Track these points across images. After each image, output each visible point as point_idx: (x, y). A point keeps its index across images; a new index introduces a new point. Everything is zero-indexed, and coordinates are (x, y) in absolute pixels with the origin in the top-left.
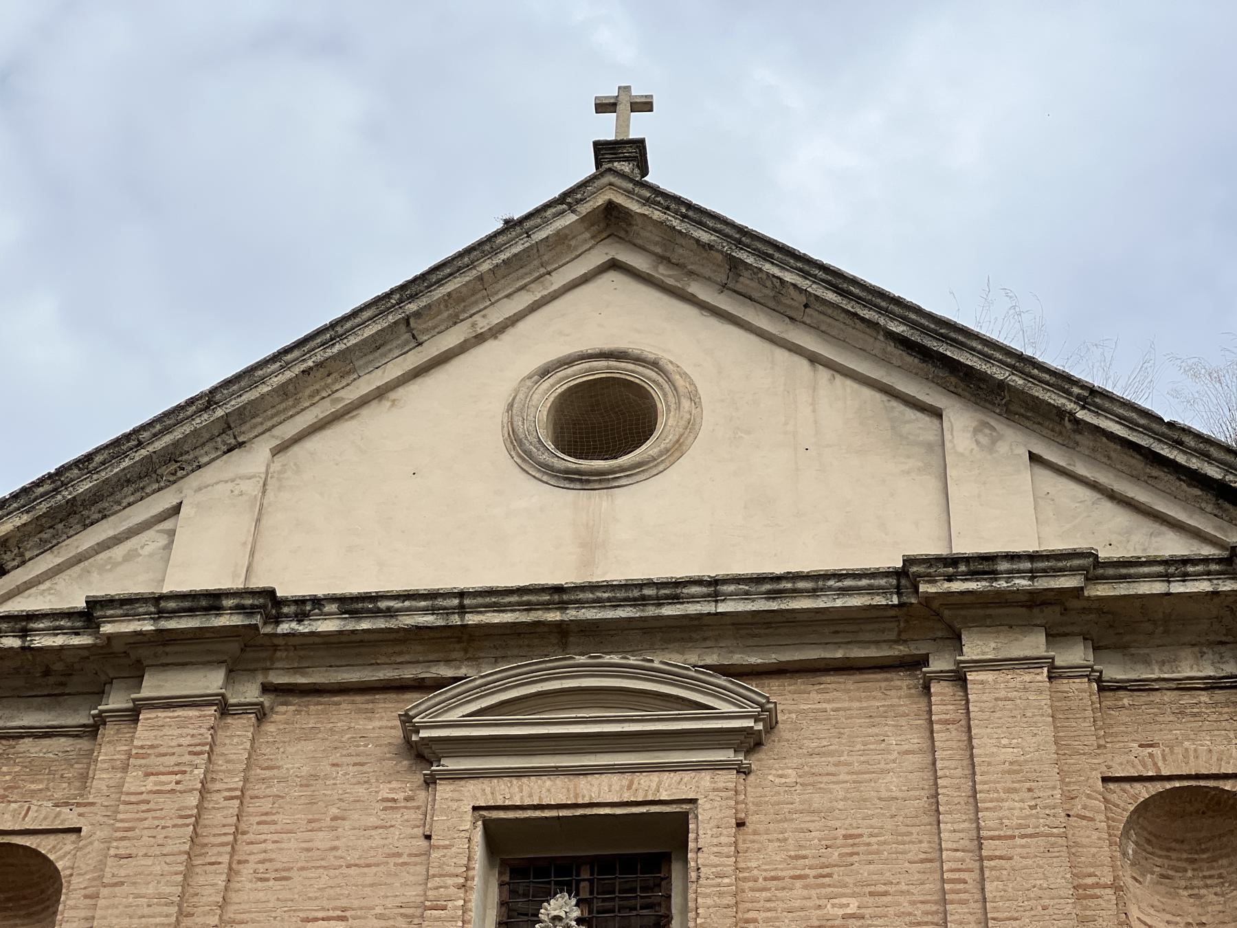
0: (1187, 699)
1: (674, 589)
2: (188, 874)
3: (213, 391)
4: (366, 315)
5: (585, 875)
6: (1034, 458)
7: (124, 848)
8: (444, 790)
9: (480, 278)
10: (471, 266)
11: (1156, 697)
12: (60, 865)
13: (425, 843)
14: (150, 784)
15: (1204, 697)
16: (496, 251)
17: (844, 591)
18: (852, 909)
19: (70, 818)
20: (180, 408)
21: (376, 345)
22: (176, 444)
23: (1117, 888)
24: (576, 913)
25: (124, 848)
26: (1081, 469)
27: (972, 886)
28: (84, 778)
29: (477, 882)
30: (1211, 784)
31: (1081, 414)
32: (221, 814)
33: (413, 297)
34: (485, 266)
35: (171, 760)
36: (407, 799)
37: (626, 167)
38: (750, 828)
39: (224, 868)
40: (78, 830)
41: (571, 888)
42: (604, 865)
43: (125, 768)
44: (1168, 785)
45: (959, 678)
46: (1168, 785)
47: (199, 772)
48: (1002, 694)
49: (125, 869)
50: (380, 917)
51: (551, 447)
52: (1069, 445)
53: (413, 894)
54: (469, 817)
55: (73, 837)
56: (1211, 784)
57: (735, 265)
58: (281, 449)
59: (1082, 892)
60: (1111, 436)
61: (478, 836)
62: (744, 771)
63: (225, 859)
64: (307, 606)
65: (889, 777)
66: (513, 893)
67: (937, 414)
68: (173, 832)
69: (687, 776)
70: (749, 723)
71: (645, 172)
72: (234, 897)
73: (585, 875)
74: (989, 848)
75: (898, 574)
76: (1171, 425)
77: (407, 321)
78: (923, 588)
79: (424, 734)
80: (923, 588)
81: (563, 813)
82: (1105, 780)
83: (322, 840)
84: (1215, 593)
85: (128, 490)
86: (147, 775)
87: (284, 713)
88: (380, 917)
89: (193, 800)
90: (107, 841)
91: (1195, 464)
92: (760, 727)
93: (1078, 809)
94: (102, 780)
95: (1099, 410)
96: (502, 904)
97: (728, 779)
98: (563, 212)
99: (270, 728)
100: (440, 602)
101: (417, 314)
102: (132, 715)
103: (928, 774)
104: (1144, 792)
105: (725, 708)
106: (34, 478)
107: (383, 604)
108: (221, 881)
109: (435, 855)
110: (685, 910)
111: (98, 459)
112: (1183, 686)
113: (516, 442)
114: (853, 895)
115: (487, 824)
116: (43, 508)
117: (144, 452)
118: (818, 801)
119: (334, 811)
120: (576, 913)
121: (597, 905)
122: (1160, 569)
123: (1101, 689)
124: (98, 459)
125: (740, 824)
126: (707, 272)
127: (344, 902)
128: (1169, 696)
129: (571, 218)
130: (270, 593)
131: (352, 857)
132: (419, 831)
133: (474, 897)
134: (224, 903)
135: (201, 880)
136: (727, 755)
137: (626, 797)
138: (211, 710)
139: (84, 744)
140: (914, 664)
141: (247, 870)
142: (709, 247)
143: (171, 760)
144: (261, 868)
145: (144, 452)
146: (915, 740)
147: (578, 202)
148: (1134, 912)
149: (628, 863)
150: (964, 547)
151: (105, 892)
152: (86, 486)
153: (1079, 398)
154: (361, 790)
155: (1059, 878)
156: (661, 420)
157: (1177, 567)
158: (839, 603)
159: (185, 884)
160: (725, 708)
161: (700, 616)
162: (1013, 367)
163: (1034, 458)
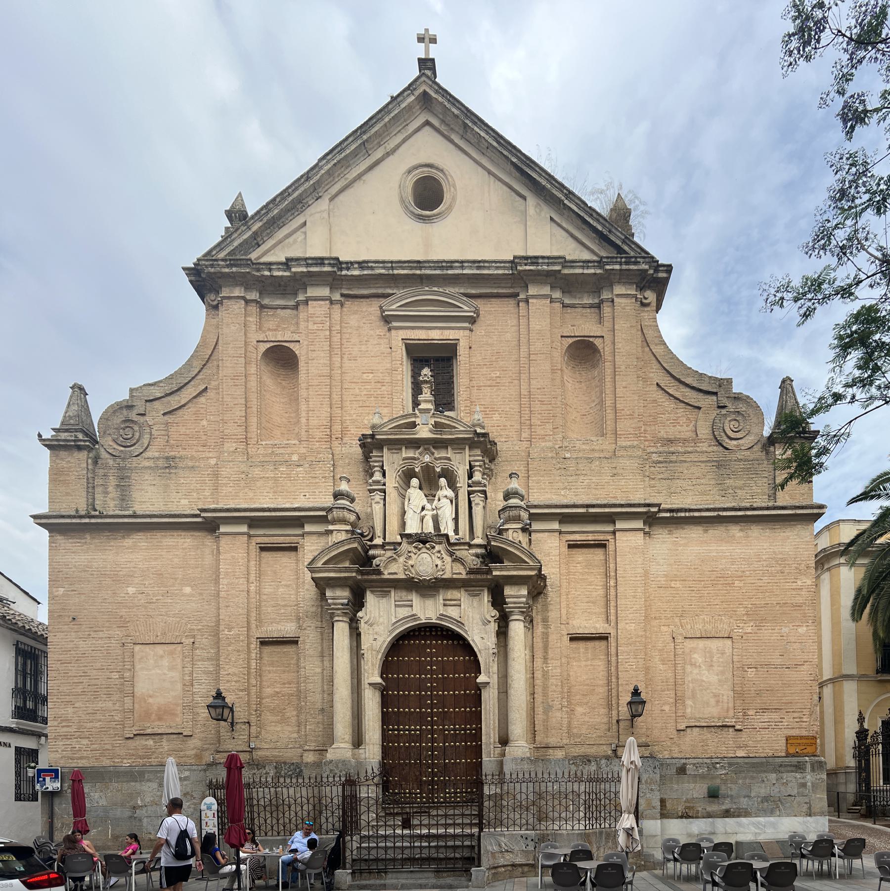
0: (584, 311)
1: (450, 264)
2: (330, 357)
3: (308, 172)
4: (351, 139)
5: (432, 362)
6: (552, 219)
7: (312, 348)
8: (393, 332)
9: (385, 125)
10: (382, 119)
11: (577, 310)
12: (296, 352)
13: (390, 350)
14: (315, 327)
15: (588, 310)
16: (389, 112)
17: (497, 268)
18: (498, 375)
19: (296, 337)
20: (298, 180)
21: (355, 154)
22: (300, 195)
23: (561, 370)
24: (430, 374)
25: (312, 348)
26: (564, 225)
27: (527, 369)
28: (297, 323)
29: (405, 363)
30: (587, 339)
31: (566, 202)
32: (336, 339)
33: (365, 132)
34: (387, 120)
35: (319, 319)
36: (384, 335)
37: (429, 73)
38: (473, 349)
39: (339, 356)
40: (299, 341)
41: (429, 366)
42: (437, 360)
43: (308, 321)
44: (577, 339)
45: (527, 302)
46: (577, 339)
47: (328, 323)
48: (538, 307)
49: (314, 355)
50: (382, 373)
51: (413, 204)
52: (562, 214)
53: (389, 365)
54: (401, 342)
55: (298, 343)
56: (587, 339)
57: (465, 126)
58: (332, 199)
59: (553, 371)
60: (573, 211)
61: (404, 348)
62: (471, 330)
63: (339, 353)
64: (350, 265)
65: (508, 334)
66: (414, 367)
67: (524, 198)
68: (324, 343)
69: (457, 331)
70: (472, 314)
71: (435, 77)
72: (343, 365)
73: (432, 362)
74: (532, 357)
75: (512, 262)
76: (590, 208)
77: (364, 143)
78: (519, 268)
79: (386, 313)
80: (519, 268)
81: (425, 342)
82: (562, 337)
83: (363, 348)
84: (595, 274)
85: (289, 214)
86: (314, 324)
87: (348, 303)
88: (382, 373)
89: (328, 333)
90: (307, 345)
91: (595, 224)
92: (475, 315)
93: (554, 346)
94: (302, 325)
95: (571, 200)
96: (412, 370)
97: (467, 332)
98: (408, 95)
99: (345, 309)
100: (386, 265)
101: (367, 140)
102: (306, 302)
103: (518, 333)
104: (571, 340)
105: (466, 308)
106: (260, 207)
107: (370, 265)
108: (339, 359)
109: (393, 354)
110: (457, 374)
111: (278, 200)
112: (584, 307)
113: (402, 201)
114: (498, 371)
115: (407, 346)
116: (265, 220)
117: (291, 198)
118: (490, 341)
119: (366, 339)
120: (430, 374)
121: (436, 372)
122: (581, 264)
123: (563, 306)
124: (278, 200)
125: (470, 348)
126: (457, 129)
127: (372, 368)
128: (579, 310)
129: (412, 98)
130: (337, 259)
131: (372, 354)
132: (388, 346)
133: (404, 367)
134: (341, 367)
135: (334, 359)
136: (466, 325)
137: (441, 338)
138: (328, 302)
139: (295, 312)
140: (515, 295)
141: (345, 357)
142: (457, 116)
143: (319, 319)
144: (349, 356)
145: (291, 198)
146: (515, 322)
147: (415, 89)
148: (565, 378)
149: (443, 359)
150: (531, 253)
151: (310, 362)
152: (276, 212)
153: (566, 195)
154: (372, 332)
155: (547, 366)
156: (445, 195)
157: (586, 263)
158: (496, 272)
159: (330, 360)
160: (466, 308)
161: (458, 275)
162: (547, 179)
163: (552, 219)
